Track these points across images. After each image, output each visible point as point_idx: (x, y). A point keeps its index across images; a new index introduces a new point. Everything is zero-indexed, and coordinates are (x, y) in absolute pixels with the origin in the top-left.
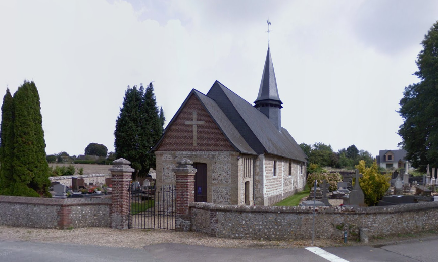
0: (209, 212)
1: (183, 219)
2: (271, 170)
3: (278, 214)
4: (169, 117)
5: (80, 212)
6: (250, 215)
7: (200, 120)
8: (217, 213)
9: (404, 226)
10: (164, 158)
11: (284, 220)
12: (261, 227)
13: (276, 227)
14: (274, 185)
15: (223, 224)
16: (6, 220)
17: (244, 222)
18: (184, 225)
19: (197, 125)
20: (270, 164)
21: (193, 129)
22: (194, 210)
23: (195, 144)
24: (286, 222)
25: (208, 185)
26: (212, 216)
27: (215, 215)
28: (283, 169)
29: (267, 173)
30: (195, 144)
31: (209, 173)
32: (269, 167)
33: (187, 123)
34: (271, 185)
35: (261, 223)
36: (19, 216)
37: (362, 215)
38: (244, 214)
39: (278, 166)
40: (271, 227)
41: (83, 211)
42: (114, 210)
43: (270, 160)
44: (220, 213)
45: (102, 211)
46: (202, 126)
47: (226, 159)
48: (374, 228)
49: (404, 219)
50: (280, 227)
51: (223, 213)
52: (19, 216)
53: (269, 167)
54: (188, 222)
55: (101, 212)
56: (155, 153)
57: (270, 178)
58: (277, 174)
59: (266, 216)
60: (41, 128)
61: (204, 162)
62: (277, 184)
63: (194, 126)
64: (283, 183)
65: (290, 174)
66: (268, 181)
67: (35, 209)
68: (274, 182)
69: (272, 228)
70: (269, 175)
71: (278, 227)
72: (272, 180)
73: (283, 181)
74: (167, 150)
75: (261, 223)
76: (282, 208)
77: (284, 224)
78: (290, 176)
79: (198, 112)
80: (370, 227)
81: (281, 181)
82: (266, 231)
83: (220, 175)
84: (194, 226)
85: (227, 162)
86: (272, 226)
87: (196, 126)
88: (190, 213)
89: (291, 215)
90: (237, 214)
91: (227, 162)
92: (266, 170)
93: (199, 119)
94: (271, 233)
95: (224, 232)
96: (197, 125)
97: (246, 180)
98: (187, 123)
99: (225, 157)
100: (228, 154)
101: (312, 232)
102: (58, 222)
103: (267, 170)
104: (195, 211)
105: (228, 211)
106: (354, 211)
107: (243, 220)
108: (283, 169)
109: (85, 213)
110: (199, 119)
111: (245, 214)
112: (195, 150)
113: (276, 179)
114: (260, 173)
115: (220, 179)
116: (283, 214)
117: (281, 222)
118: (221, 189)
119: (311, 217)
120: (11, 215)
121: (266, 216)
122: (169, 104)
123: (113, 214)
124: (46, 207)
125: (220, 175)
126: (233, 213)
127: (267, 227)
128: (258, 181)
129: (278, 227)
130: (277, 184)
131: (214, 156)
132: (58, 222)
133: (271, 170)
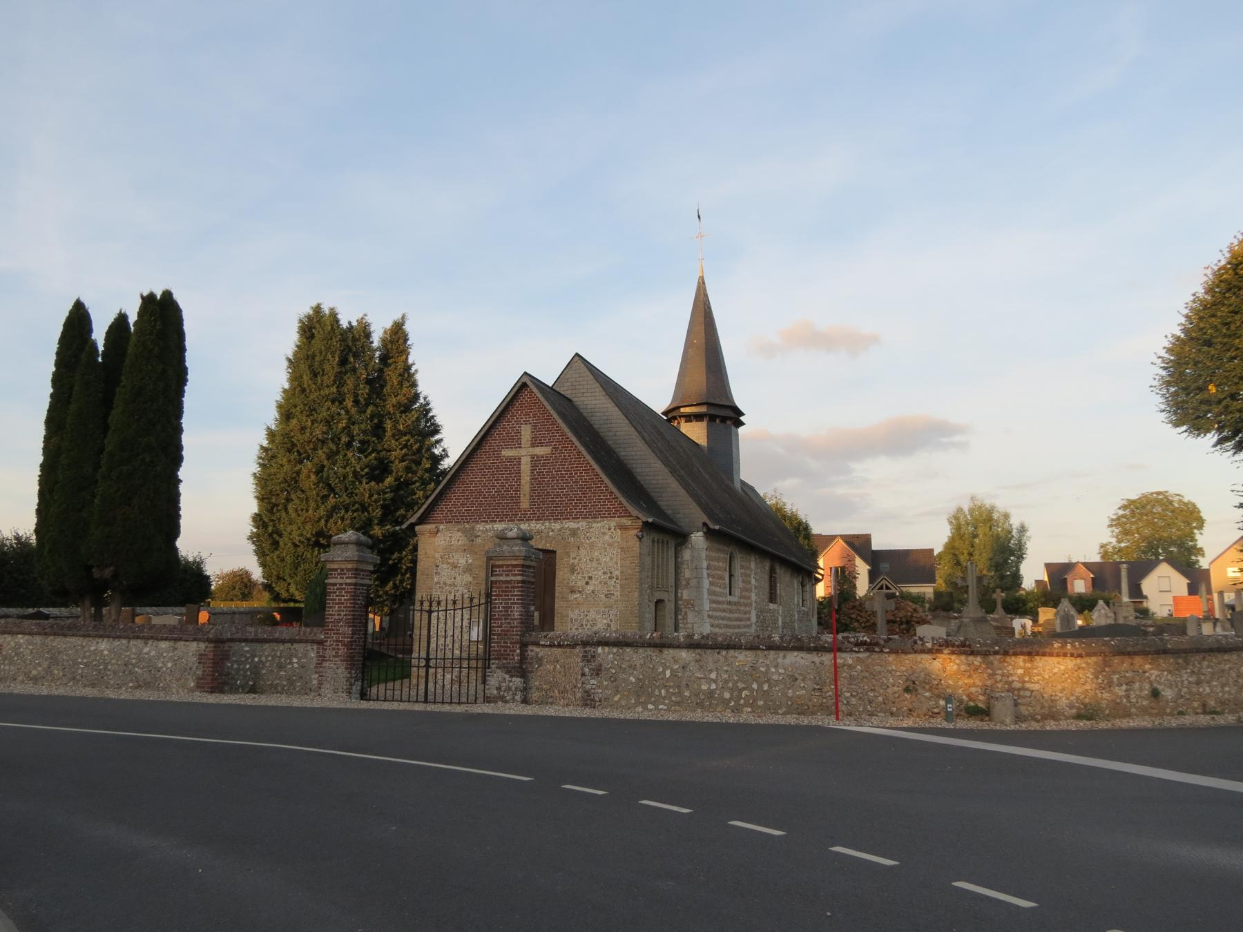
0: (578, 650)
1: (507, 673)
2: (721, 578)
3: (759, 652)
4: (454, 441)
5: (247, 659)
6: (684, 654)
7: (541, 444)
8: (600, 650)
9: (1117, 696)
10: (440, 541)
11: (776, 666)
12: (713, 686)
13: (755, 686)
14: (729, 619)
15: (613, 679)
16: (74, 678)
17: (668, 673)
18: (509, 689)
19: (532, 457)
20: (718, 560)
21: (522, 467)
22: (537, 649)
23: (525, 504)
24: (780, 674)
25: (559, 604)
26: (587, 659)
27: (593, 657)
28: (753, 581)
29: (711, 584)
30: (525, 504)
31: (561, 574)
32: (718, 568)
33: (507, 453)
34: (723, 619)
35: (713, 676)
36: (106, 668)
37: (991, 658)
38: (669, 653)
39: (738, 572)
40: (740, 685)
41: (253, 656)
42: (329, 653)
43: (719, 551)
44: (606, 649)
45: (299, 659)
46: (546, 459)
47: (607, 538)
48: (1028, 694)
49: (1115, 677)
50: (766, 687)
51: (615, 650)
52: (106, 668)
53: (718, 568)
54: (517, 681)
55: (295, 660)
56: (417, 528)
57: (720, 599)
58: (737, 592)
59: (726, 658)
60: (180, 440)
61: (548, 547)
62: (737, 619)
63: (523, 460)
64: (754, 619)
65: (773, 598)
66: (714, 605)
67: (146, 650)
68: (731, 612)
69: (744, 689)
70: (718, 589)
71: (760, 686)
72: (725, 606)
73: (754, 613)
74: (455, 519)
75: (713, 676)
76: (770, 637)
77: (775, 677)
78: (772, 606)
79: (535, 427)
80: (1019, 690)
81: (750, 613)
82: (727, 695)
83: (590, 578)
84: (534, 690)
85: (610, 545)
86: (744, 682)
87: (529, 459)
88: (522, 655)
89: (796, 653)
90: (649, 651)
91: (610, 545)
92: (709, 575)
93: (535, 443)
94: (742, 702)
95: (616, 699)
96: (532, 457)
97: (658, 595)
98: (507, 453)
99: (604, 534)
100: (613, 524)
101: (854, 701)
102: (199, 679)
103: (713, 576)
104: (537, 654)
105: (628, 645)
106: (970, 646)
107: (665, 668)
108: (753, 581)
109: (260, 661)
110: (535, 443)
111: (671, 651)
112: (526, 518)
113: (736, 604)
114: (693, 582)
115: (590, 588)
116: (772, 652)
117: (767, 672)
118: (592, 615)
119: (850, 661)
120: (86, 665)
121: (726, 658)
122: (458, 402)
123: (325, 664)
124: (172, 643)
125: (590, 578)
126: (641, 650)
127: (730, 685)
128: (688, 602)
129: (760, 686)
130: (737, 619)
131: (574, 533)
132: (199, 679)
133: (721, 578)
